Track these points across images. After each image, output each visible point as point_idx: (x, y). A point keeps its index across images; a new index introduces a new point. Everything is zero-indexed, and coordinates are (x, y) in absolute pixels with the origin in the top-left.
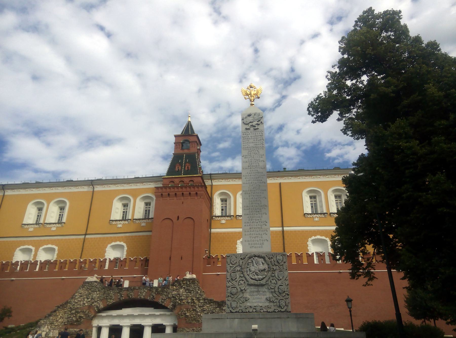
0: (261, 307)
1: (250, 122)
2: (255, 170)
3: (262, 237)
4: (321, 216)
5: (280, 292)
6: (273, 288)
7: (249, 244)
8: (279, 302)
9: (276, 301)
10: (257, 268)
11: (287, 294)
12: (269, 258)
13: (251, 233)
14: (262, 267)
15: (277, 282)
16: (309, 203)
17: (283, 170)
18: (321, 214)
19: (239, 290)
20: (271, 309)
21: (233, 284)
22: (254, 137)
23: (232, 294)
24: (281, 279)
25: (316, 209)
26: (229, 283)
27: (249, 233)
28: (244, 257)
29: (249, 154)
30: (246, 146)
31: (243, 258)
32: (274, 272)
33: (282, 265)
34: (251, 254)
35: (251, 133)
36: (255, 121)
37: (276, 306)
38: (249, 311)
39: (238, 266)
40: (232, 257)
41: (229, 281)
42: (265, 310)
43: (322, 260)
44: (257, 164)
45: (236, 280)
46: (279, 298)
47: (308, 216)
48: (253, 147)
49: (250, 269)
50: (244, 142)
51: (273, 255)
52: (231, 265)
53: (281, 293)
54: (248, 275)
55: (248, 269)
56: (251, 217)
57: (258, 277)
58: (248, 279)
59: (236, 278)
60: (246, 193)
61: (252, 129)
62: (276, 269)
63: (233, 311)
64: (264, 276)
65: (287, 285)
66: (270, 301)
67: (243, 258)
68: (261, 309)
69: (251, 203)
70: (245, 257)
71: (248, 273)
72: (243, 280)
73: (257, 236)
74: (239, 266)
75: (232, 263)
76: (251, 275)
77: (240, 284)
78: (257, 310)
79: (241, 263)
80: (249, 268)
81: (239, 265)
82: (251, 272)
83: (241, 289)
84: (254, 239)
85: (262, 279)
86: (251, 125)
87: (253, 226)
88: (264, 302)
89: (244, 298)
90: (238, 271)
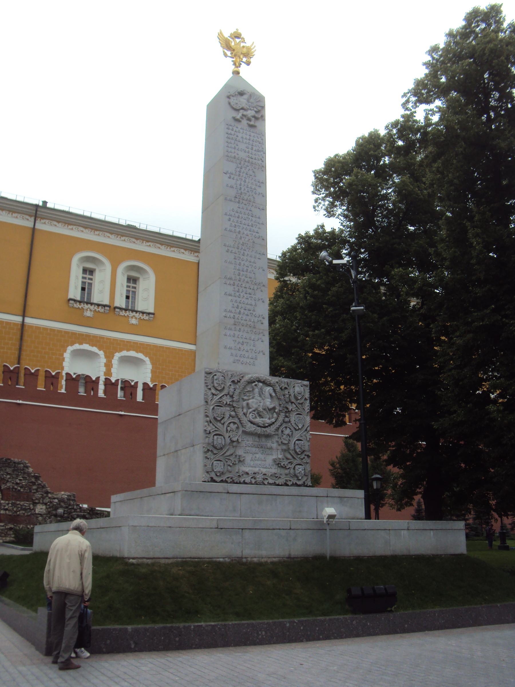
0: (264, 474)
1: (242, 109)
2: (247, 209)
3: (254, 346)
4: (97, 310)
5: (298, 451)
6: (286, 442)
7: (232, 355)
8: (294, 468)
9: (289, 466)
10: (261, 404)
11: (308, 456)
12: (281, 388)
13: (235, 332)
14: (269, 403)
15: (292, 433)
16: (80, 280)
17: (41, 204)
18: (99, 305)
19: (228, 441)
20: (280, 479)
21: (216, 429)
22: (248, 141)
23: (215, 448)
24: (299, 429)
25: (90, 294)
26: (209, 425)
27: (232, 333)
28: (239, 380)
29: (238, 173)
30: (233, 155)
31: (236, 381)
32: (287, 415)
33: (302, 404)
34: (250, 376)
35: (241, 131)
36: (251, 109)
37: (289, 475)
38: (244, 481)
39: (226, 395)
40: (215, 375)
41: (211, 422)
42: (271, 481)
43: (93, 389)
44: (252, 200)
45: (222, 422)
46: (295, 462)
47: (75, 305)
48: (245, 161)
49: (248, 404)
50: (230, 145)
51: (287, 384)
52: (213, 391)
53: (300, 453)
54: (245, 414)
55: (245, 403)
56: (236, 301)
57: (263, 421)
58: (245, 422)
59: (223, 418)
60: (228, 250)
61: (245, 122)
62: (291, 410)
63: (215, 478)
64: (273, 420)
65: (308, 439)
66: (280, 465)
67: (236, 381)
68: (264, 479)
69: (237, 272)
70: (240, 380)
71: (245, 411)
72: (234, 423)
73: (245, 341)
74: (228, 396)
75: (217, 388)
76: (251, 417)
77: (229, 429)
78: (257, 479)
79: (232, 390)
80: (247, 402)
81: (228, 393)
82: (251, 410)
83: (231, 439)
84: (240, 345)
85: (270, 425)
86: (243, 115)
87: (240, 321)
88: (269, 467)
89: (236, 456)
90: (226, 404)
